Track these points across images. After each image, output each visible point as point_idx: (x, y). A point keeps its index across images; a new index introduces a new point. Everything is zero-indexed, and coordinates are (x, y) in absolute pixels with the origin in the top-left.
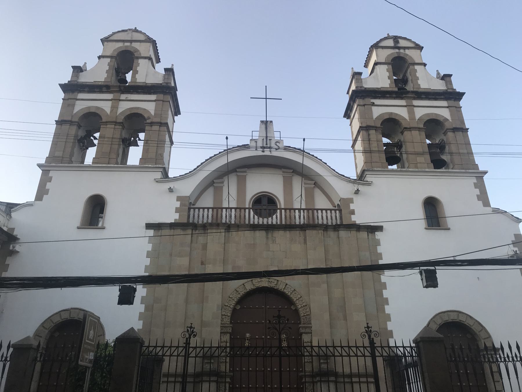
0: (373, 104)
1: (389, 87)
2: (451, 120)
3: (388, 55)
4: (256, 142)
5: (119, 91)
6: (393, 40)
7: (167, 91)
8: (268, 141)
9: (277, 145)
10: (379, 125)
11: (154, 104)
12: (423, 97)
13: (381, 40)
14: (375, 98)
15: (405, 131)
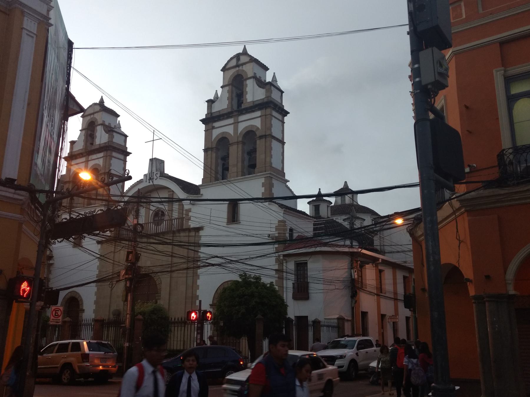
0: (213, 128)
1: (227, 107)
2: (260, 128)
3: (231, 76)
4: (146, 176)
5: (87, 155)
6: (237, 59)
7: (107, 149)
8: (152, 173)
9: (156, 176)
10: (214, 146)
11: (102, 159)
12: (244, 112)
13: (229, 61)
14: (215, 121)
15: (231, 146)
